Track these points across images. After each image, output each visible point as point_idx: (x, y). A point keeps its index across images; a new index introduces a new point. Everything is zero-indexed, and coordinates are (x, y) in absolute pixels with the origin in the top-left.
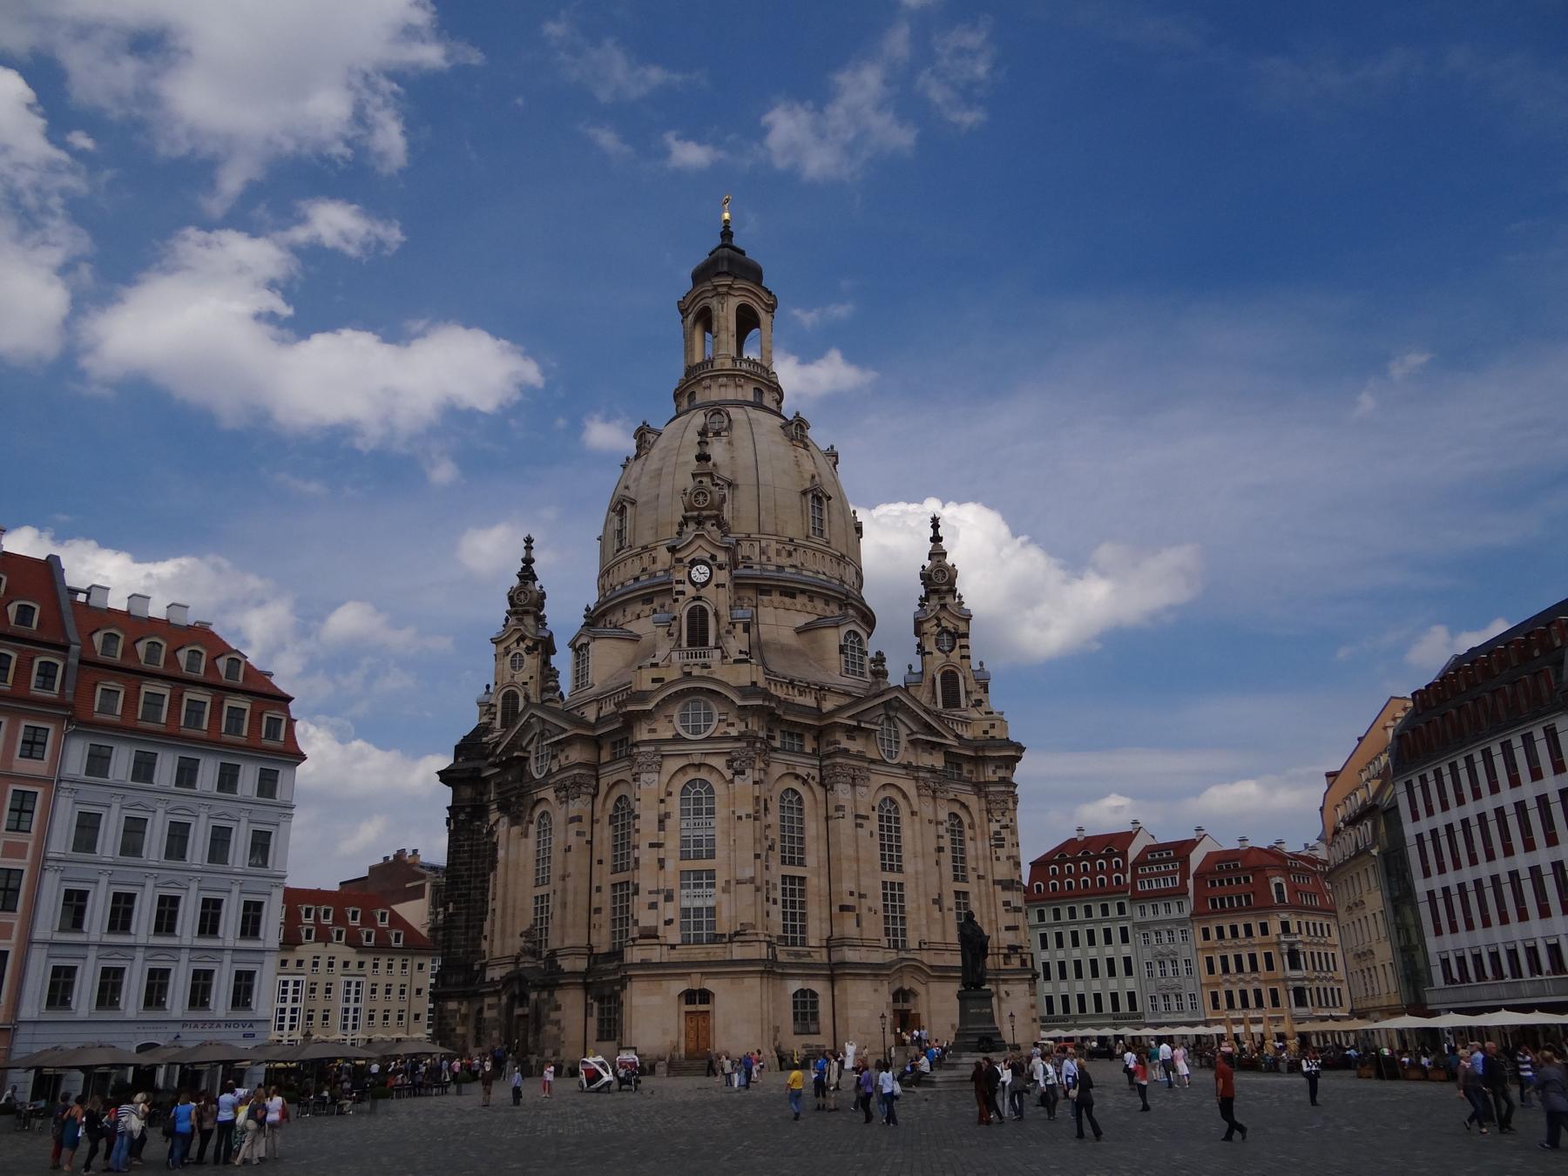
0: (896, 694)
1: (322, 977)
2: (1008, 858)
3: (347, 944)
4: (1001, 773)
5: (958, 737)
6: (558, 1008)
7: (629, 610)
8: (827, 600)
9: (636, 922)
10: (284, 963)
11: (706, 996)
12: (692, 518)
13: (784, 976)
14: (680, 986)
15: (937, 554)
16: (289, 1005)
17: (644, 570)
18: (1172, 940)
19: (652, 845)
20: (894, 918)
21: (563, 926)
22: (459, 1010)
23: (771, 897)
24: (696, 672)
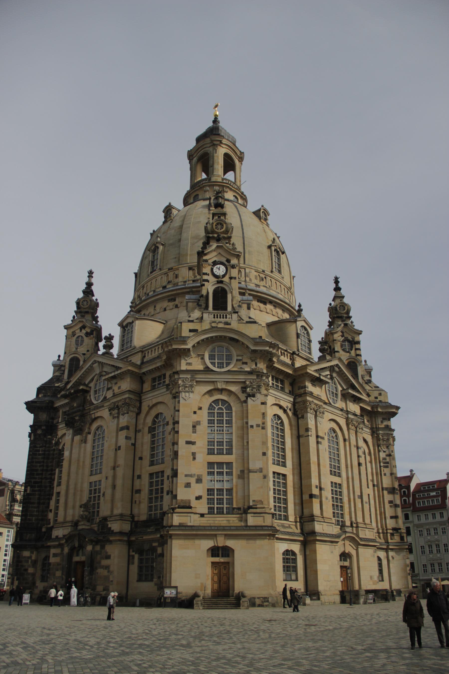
2: (392, 474)
4: (385, 423)
6: (108, 557)
7: (158, 306)
8: (284, 309)
9: (175, 497)
11: (227, 552)
12: (213, 238)
13: (278, 539)
14: (210, 543)
15: (338, 297)
17: (169, 282)
18: (436, 533)
19: (188, 443)
20: (337, 506)
21: (113, 501)
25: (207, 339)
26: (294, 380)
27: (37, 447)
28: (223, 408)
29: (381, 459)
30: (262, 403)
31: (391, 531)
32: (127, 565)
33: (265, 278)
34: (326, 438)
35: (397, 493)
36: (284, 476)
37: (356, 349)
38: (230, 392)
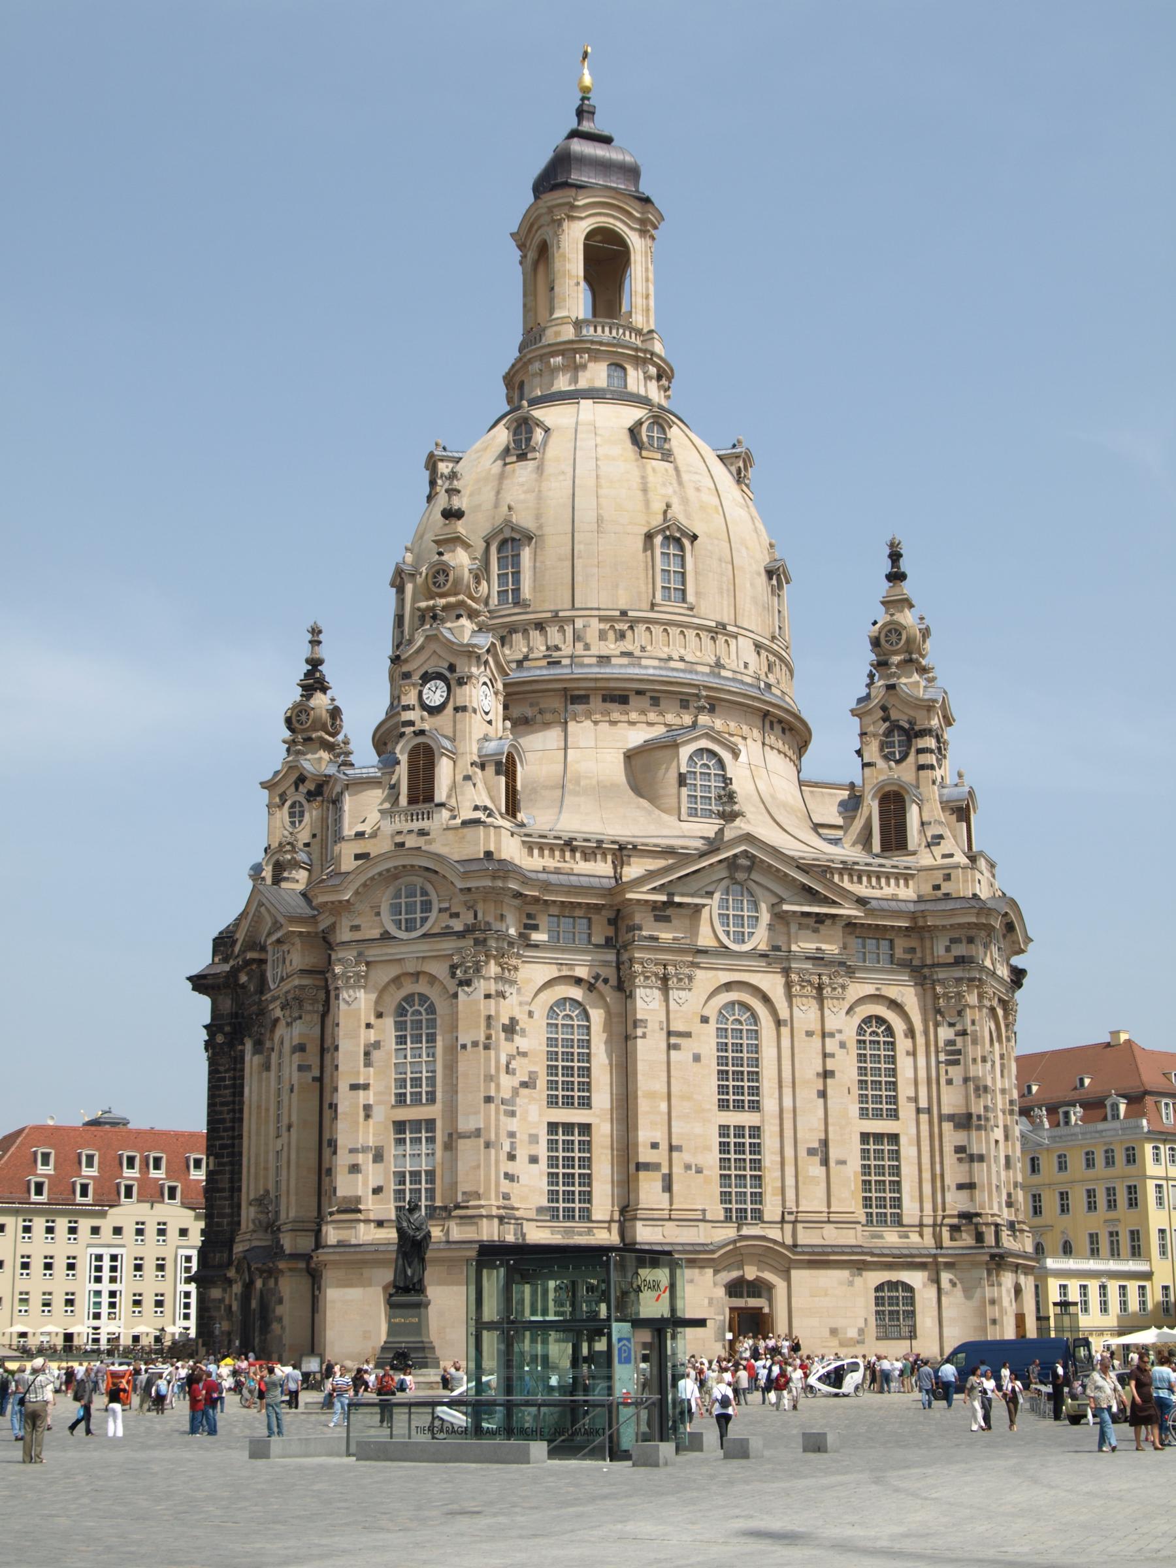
0: (743, 848)
1: (151, 1249)
2: (966, 1080)
3: (184, 1205)
5: (861, 901)
10: (95, 1230)
16: (105, 1287)
19: (354, 1087)
22: (222, 1300)
23: (522, 1154)
24: (411, 842)
25: (380, 874)
26: (618, 911)
27: (220, 1072)
28: (422, 1010)
29: (941, 1044)
30: (488, 996)
31: (955, 1221)
32: (310, 1315)
33: (631, 628)
34: (712, 1026)
35: (979, 1128)
36: (586, 1128)
37: (920, 751)
38: (433, 979)
